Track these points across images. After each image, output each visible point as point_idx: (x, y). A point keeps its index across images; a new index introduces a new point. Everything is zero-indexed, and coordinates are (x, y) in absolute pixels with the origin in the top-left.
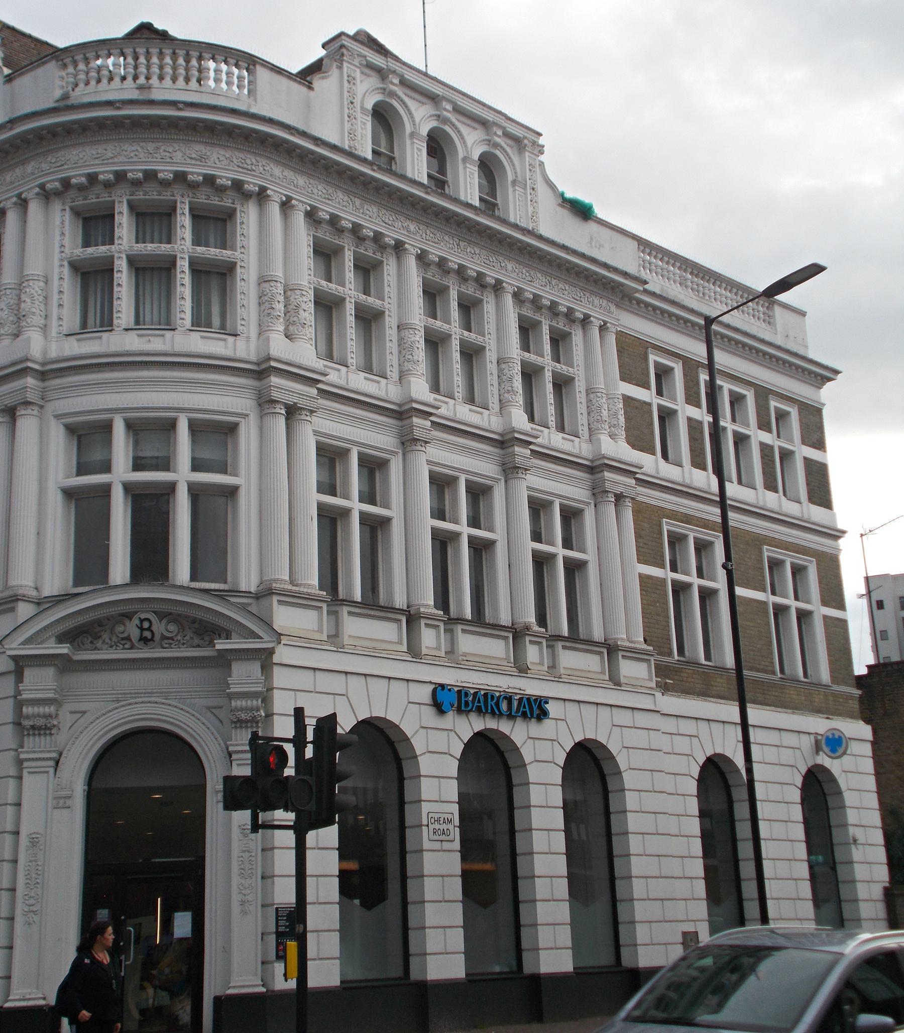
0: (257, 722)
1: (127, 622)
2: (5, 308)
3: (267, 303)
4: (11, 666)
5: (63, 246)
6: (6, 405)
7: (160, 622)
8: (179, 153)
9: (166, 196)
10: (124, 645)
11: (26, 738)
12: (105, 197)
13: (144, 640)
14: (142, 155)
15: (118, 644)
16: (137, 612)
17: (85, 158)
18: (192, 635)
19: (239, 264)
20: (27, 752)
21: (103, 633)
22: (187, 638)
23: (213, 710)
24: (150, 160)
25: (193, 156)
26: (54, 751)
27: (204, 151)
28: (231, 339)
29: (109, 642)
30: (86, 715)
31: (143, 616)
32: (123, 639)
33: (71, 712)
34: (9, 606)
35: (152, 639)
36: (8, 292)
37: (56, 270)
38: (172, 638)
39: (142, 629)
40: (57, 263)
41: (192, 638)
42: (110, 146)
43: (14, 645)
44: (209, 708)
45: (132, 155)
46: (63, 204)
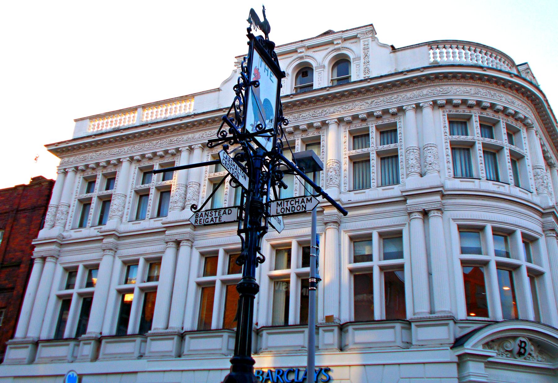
1: (512, 341)
2: (414, 159)
3: (540, 179)
4: (456, 359)
5: (446, 132)
6: (424, 209)
8: (503, 98)
9: (496, 117)
12: (467, 112)
13: (520, 354)
14: (488, 95)
16: (520, 336)
17: (460, 92)
19: (526, 157)
24: (492, 98)
25: (509, 101)
27: (513, 100)
28: (530, 194)
31: (523, 339)
32: (507, 351)
34: (446, 322)
35: (523, 354)
36: (415, 151)
37: (444, 144)
39: (520, 347)
40: (444, 141)
42: (473, 88)
43: (469, 347)
45: (484, 94)
46: (444, 112)
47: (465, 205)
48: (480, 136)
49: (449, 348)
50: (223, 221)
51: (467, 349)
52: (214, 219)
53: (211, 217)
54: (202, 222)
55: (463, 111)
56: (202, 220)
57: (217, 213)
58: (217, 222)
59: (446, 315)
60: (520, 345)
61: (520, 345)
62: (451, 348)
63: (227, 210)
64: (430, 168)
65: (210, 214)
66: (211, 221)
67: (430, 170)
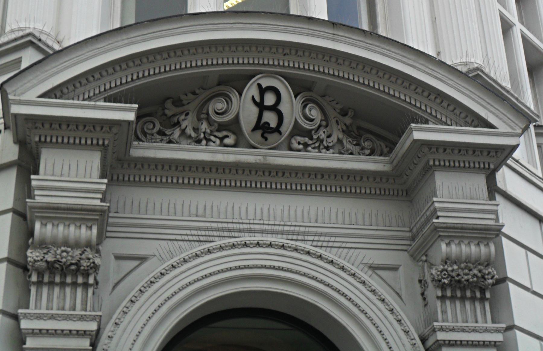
0: (483, 291)
1: (234, 96)
7: (296, 97)
10: (222, 139)
11: (33, 290)
15: (212, 138)
18: (341, 136)
20: (39, 317)
21: (183, 117)
22: (334, 138)
23: (380, 272)
26: (93, 318)
29: (193, 134)
30: (146, 265)
31: (266, 83)
32: (221, 127)
33: (118, 257)
35: (277, 130)
38: (308, 134)
39: (261, 106)
41: (340, 141)
44: (374, 268)
60: (258, 99)
61: (258, 99)
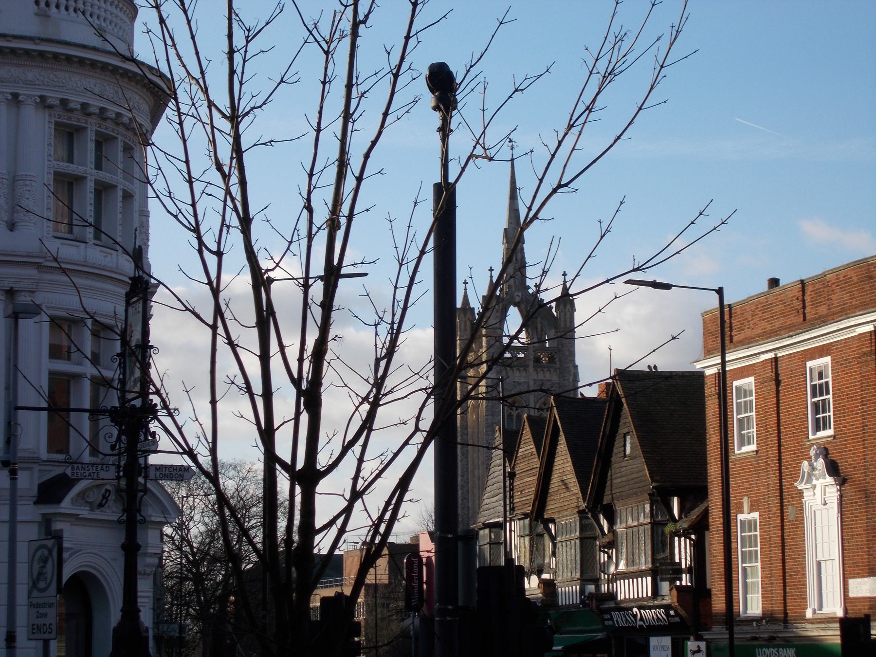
4: (39, 519)
5: (50, 155)
32: (87, 502)
39: (104, 497)
46: (50, 115)
47: (64, 285)
48: (93, 167)
49: (31, 503)
50: (101, 478)
51: (62, 508)
52: (92, 474)
53: (88, 472)
54: (79, 475)
55: (76, 119)
56: (79, 474)
57: (94, 468)
58: (95, 477)
59: (31, 455)
62: (35, 503)
63: (104, 466)
64: (27, 218)
65: (86, 469)
66: (89, 476)
67: (25, 221)
